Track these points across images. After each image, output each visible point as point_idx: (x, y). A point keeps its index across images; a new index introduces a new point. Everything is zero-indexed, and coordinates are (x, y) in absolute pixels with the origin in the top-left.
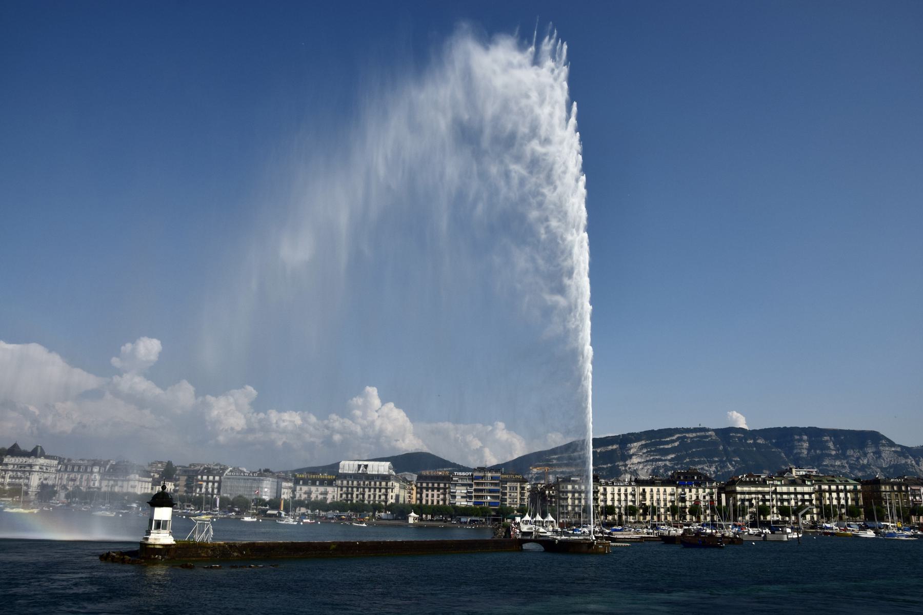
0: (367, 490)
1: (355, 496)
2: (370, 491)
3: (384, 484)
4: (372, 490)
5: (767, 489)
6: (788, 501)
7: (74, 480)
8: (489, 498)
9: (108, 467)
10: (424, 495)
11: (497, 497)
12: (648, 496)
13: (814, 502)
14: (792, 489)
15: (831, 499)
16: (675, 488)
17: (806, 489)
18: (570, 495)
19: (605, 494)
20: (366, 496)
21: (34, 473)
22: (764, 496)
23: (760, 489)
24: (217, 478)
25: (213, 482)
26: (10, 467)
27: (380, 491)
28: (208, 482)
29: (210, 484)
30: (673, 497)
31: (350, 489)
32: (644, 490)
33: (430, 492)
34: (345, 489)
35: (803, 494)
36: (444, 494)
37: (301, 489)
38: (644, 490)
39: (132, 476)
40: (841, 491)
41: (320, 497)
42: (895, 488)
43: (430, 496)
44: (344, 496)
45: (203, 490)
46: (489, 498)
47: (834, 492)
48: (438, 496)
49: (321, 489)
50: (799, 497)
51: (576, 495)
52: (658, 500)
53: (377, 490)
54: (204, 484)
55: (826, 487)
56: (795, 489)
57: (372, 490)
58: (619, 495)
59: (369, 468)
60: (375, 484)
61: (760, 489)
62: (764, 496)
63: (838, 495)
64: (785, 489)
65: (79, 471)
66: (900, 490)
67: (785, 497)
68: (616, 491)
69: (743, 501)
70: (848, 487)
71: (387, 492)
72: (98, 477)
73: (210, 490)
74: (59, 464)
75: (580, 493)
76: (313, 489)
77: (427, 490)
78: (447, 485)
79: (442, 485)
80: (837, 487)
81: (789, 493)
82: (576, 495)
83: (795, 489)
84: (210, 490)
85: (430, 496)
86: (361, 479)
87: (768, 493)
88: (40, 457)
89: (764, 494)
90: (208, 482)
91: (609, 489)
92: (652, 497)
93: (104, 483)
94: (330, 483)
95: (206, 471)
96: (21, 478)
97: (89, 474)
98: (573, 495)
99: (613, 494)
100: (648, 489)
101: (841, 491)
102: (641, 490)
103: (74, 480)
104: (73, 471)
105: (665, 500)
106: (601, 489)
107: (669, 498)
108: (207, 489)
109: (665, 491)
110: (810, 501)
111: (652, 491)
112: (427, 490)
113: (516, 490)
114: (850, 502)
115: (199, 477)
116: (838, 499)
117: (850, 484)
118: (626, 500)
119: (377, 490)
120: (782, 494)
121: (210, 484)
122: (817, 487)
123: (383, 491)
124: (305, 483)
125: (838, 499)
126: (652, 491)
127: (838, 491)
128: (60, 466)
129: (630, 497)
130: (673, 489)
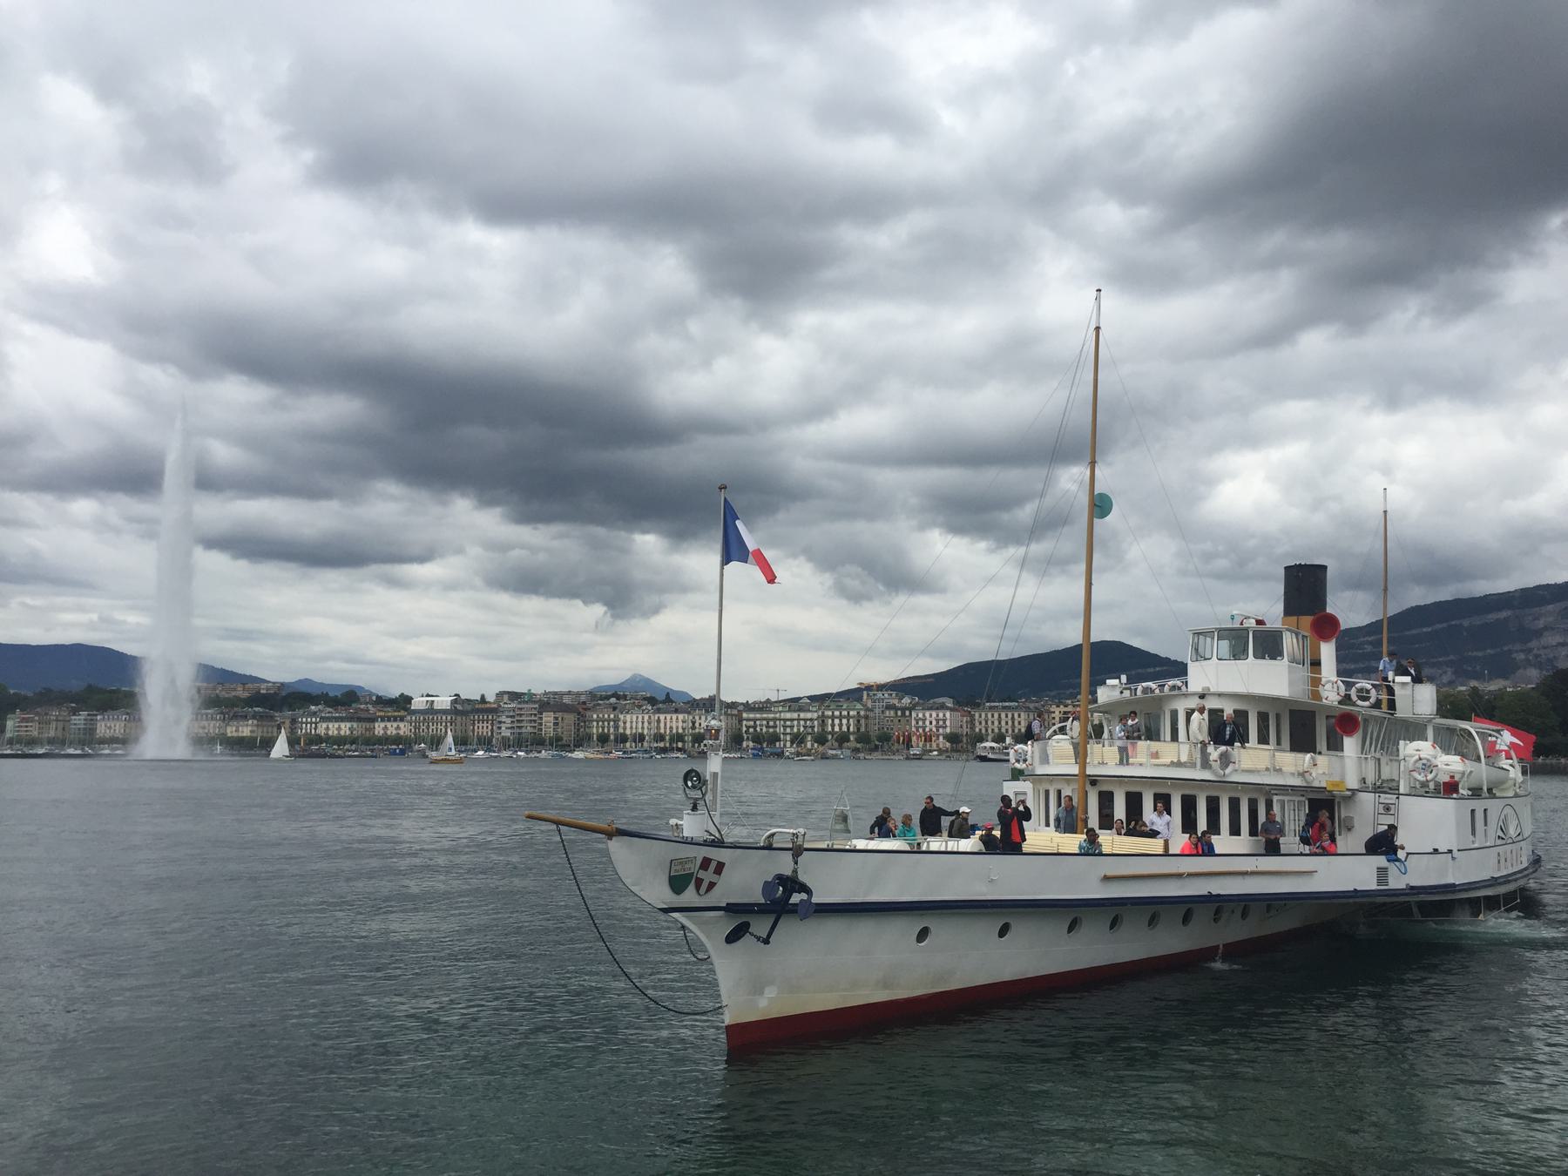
0: (431, 724)
1: (421, 730)
5: (771, 716)
6: (792, 727)
8: (528, 728)
9: (231, 715)
10: (476, 728)
11: (535, 727)
12: (662, 725)
13: (816, 730)
14: (795, 715)
15: (833, 725)
16: (686, 715)
17: (809, 715)
19: (625, 723)
20: (430, 730)
22: (768, 723)
23: (765, 716)
25: (311, 723)
28: (307, 723)
29: (309, 725)
30: (684, 725)
33: (481, 725)
34: (413, 724)
35: (805, 720)
36: (492, 725)
37: (379, 726)
39: (250, 722)
40: (845, 717)
41: (394, 732)
42: (899, 713)
43: (481, 728)
44: (413, 730)
45: (304, 731)
46: (528, 728)
47: (837, 718)
48: (487, 727)
49: (395, 725)
50: (802, 723)
51: (600, 723)
52: (671, 728)
54: (304, 725)
55: (830, 713)
56: (799, 715)
59: (435, 704)
61: (765, 716)
62: (768, 723)
63: (841, 720)
64: (788, 715)
65: (207, 720)
66: (903, 714)
67: (788, 723)
68: (634, 719)
69: (748, 727)
70: (852, 713)
71: (446, 725)
75: (603, 722)
76: (389, 725)
78: (495, 717)
79: (490, 717)
80: (841, 713)
81: (792, 720)
82: (600, 723)
83: (799, 715)
84: (309, 731)
85: (481, 728)
86: (426, 714)
87: (771, 720)
89: (768, 720)
90: (307, 723)
91: (628, 717)
92: (665, 725)
94: (402, 720)
98: (598, 724)
99: (631, 722)
100: (662, 717)
101: (845, 717)
102: (656, 718)
104: (202, 720)
105: (677, 728)
106: (621, 717)
107: (680, 724)
108: (306, 730)
109: (677, 719)
110: (813, 727)
111: (666, 718)
114: (851, 729)
115: (300, 720)
116: (841, 725)
117: (853, 710)
118: (643, 728)
120: (785, 720)
121: (309, 725)
122: (820, 713)
123: (444, 724)
124: (382, 720)
125: (841, 725)
126: (666, 718)
127: (841, 718)
129: (646, 725)
130: (684, 717)
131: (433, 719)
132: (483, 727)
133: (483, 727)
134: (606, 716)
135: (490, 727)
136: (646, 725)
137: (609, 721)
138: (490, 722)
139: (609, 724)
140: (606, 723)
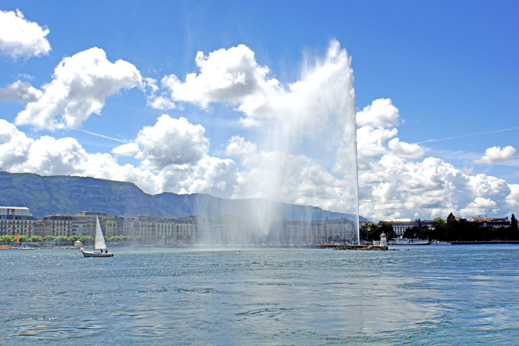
0: (16, 226)
2: (18, 227)
3: (28, 221)
4: (20, 226)
10: (55, 229)
18: (140, 228)
27: (26, 227)
31: (4, 226)
32: (178, 225)
33: (59, 227)
38: (178, 225)
43: (59, 230)
53: (24, 226)
57: (20, 226)
58: (166, 228)
60: (22, 221)
77: (58, 226)
85: (59, 230)
102: (176, 226)
112: (58, 226)
113: (111, 225)
119: (24, 226)
123: (28, 226)
130: (191, 226)
131: (18, 223)
132: (61, 230)
133: (61, 230)
134: (147, 224)
135: (67, 229)
136: (171, 229)
137: (149, 226)
138: (67, 226)
139: (149, 229)
140: (147, 228)
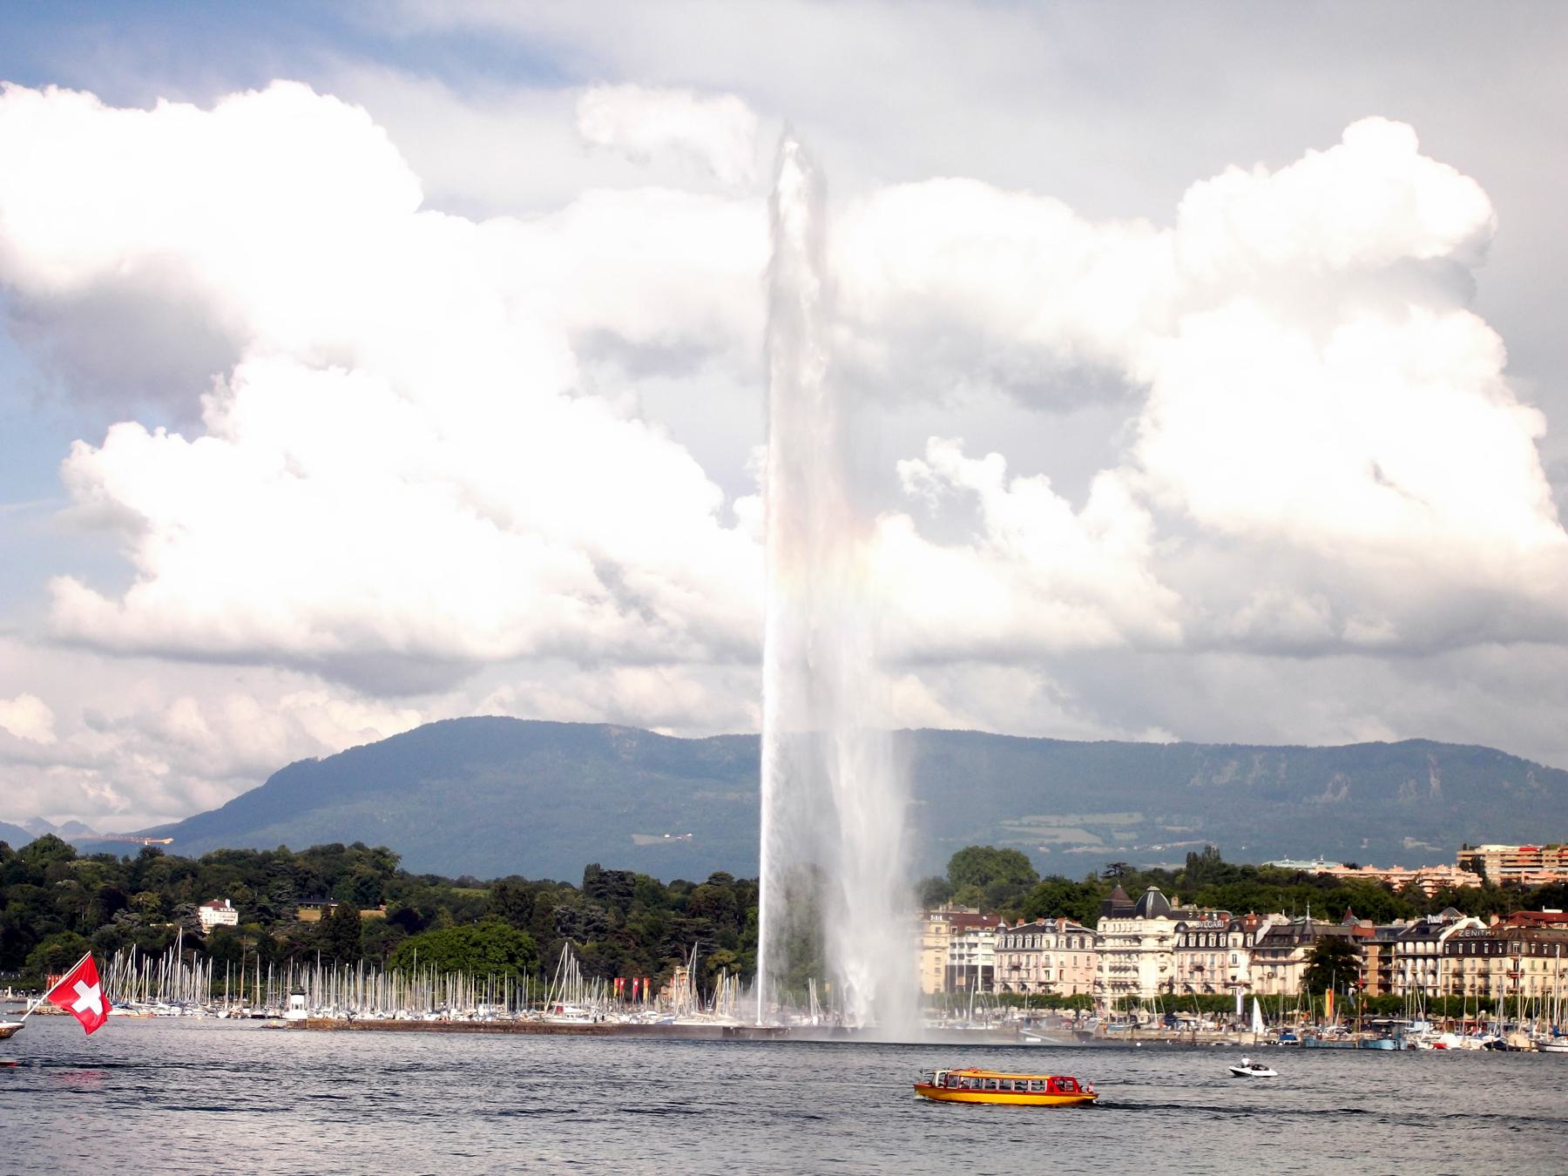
7: (1200, 969)
9: (1261, 933)
21: (1144, 954)
24: (1430, 945)
26: (1109, 944)
28: (1415, 958)
65: (1207, 947)
72: (1244, 958)
73: (1420, 976)
74: (1177, 930)
88: (1153, 917)
93: (1257, 971)
95: (1415, 930)
96: (1126, 969)
97: (1224, 953)
103: (1200, 969)
115: (1400, 945)
128: (1178, 935)
